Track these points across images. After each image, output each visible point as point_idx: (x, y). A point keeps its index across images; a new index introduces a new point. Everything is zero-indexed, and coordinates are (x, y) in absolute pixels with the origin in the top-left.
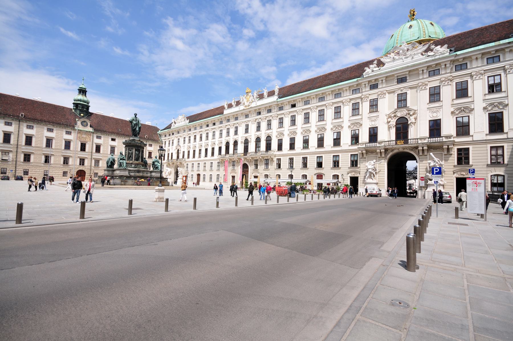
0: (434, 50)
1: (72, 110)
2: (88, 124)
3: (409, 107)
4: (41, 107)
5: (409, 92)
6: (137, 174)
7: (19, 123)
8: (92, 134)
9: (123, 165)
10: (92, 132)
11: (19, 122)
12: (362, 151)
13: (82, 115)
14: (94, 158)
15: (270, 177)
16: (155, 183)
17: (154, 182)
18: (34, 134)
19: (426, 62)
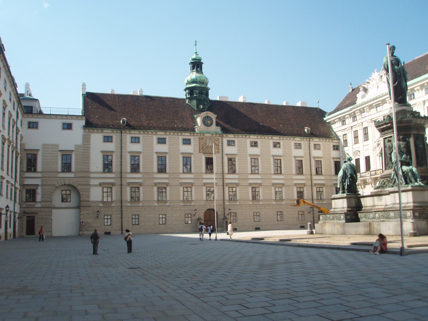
4: (145, 104)
7: (121, 136)
8: (220, 138)
11: (121, 133)
18: (140, 150)
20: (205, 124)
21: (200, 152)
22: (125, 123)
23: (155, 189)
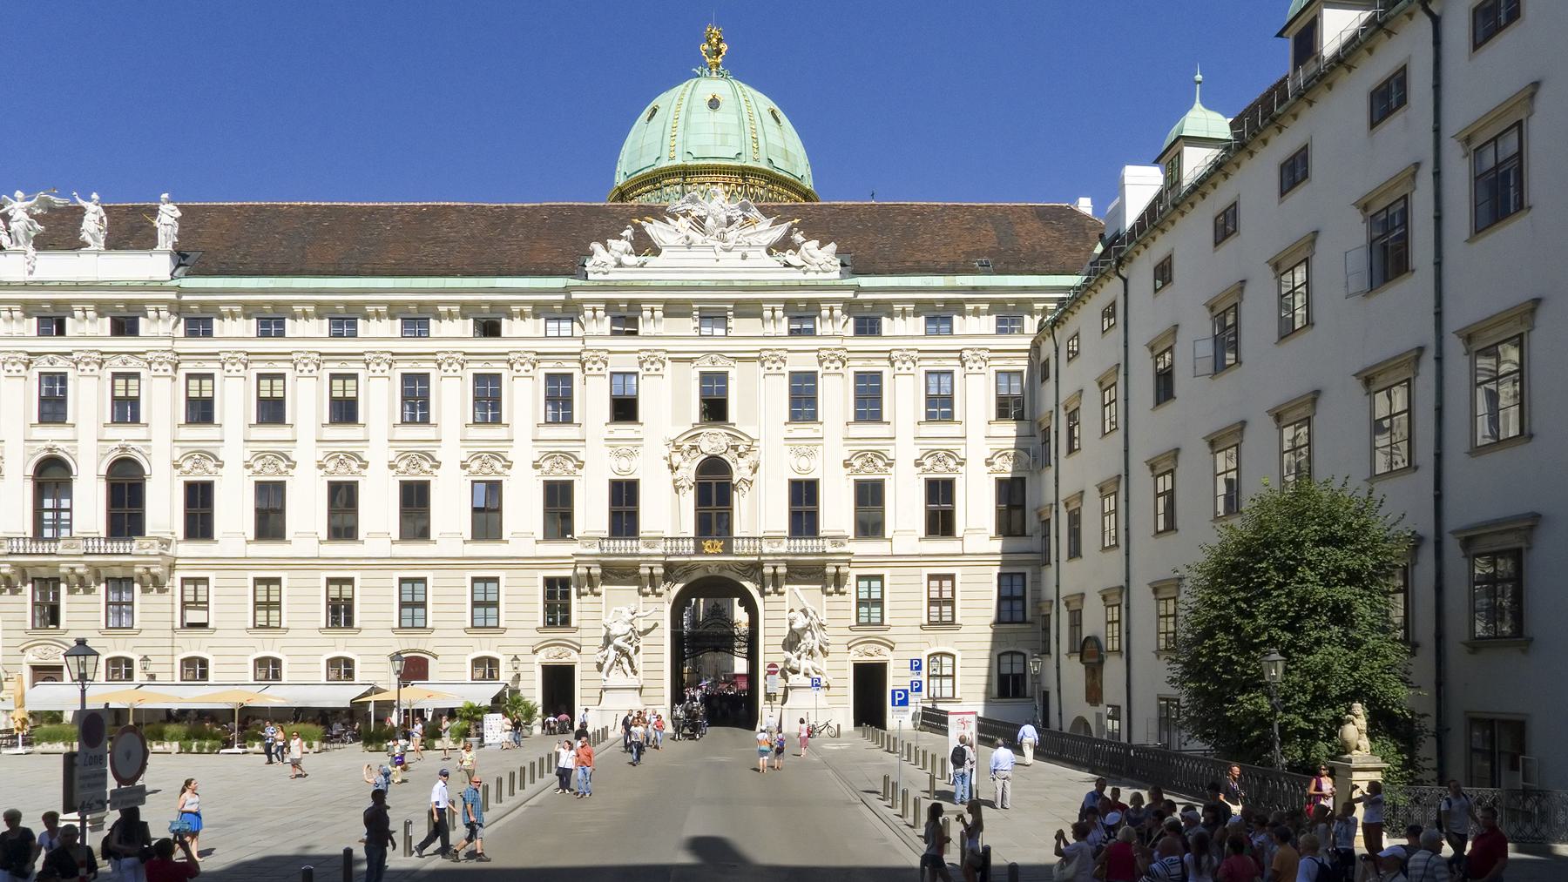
0: (802, 248)
3: (734, 424)
5: (736, 374)
12: (589, 568)
15: (152, 669)
19: (783, 288)
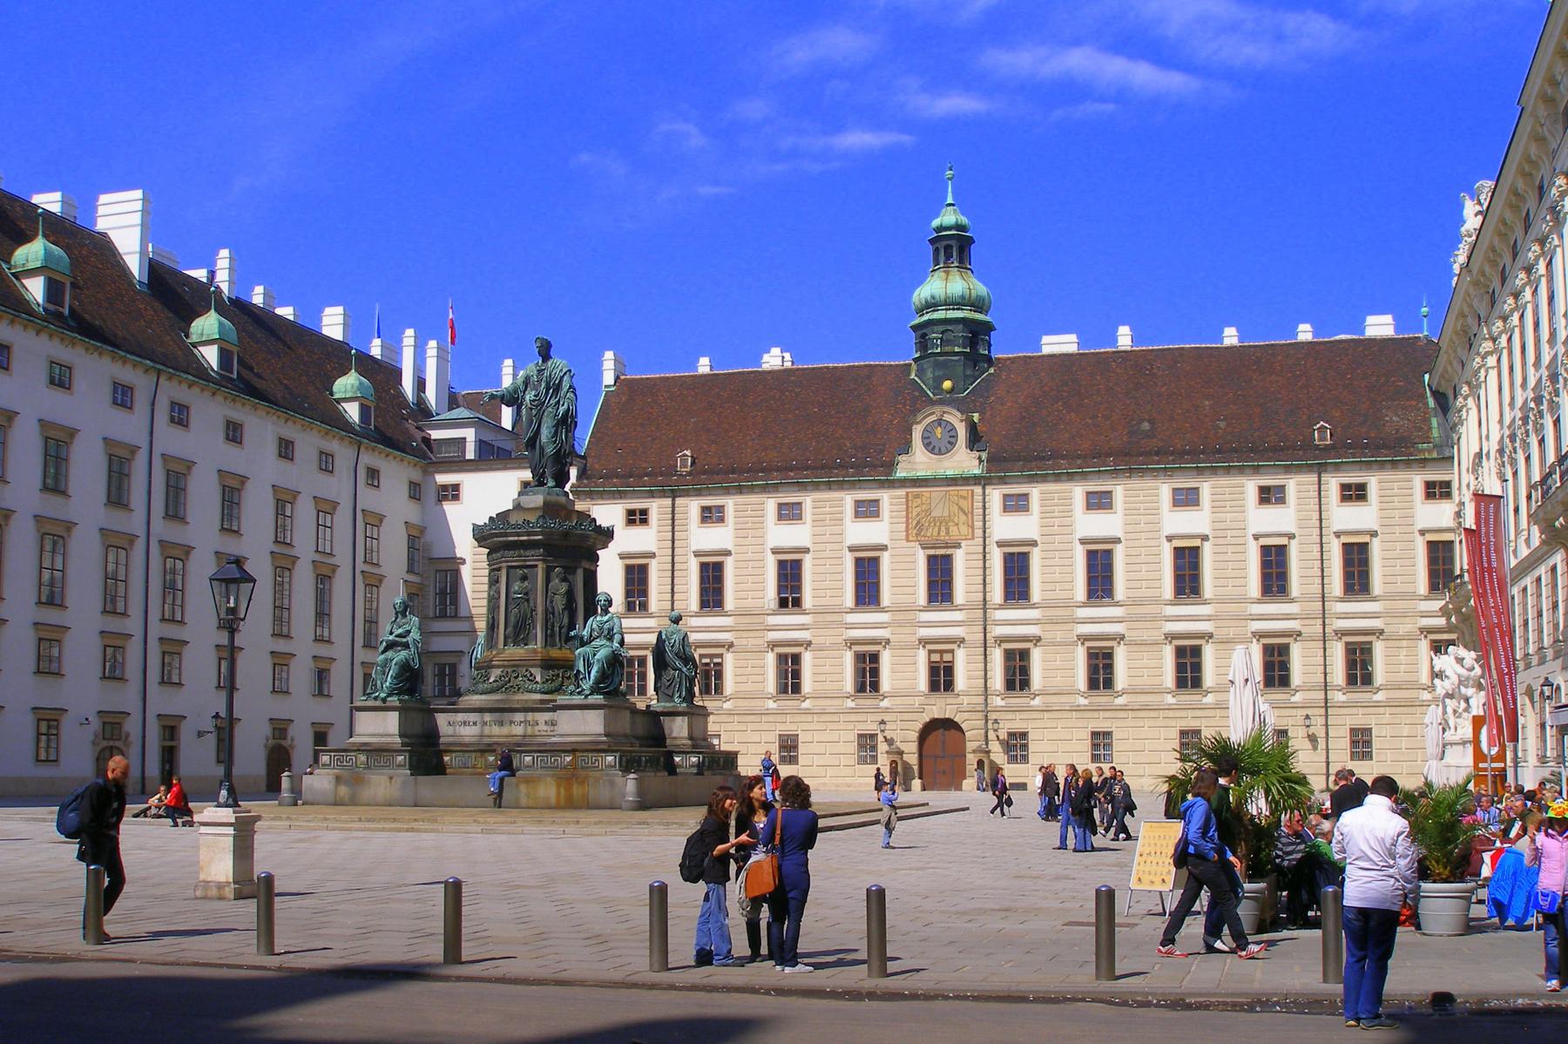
1: (909, 374)
2: (955, 437)
6: (496, 730)
7: (673, 505)
8: (978, 490)
9: (379, 682)
10: (976, 480)
13: (947, 384)
14: (1001, 640)
16: (523, 788)
17: (517, 785)
20: (932, 446)
21: (908, 541)
22: (686, 466)
23: (771, 659)
